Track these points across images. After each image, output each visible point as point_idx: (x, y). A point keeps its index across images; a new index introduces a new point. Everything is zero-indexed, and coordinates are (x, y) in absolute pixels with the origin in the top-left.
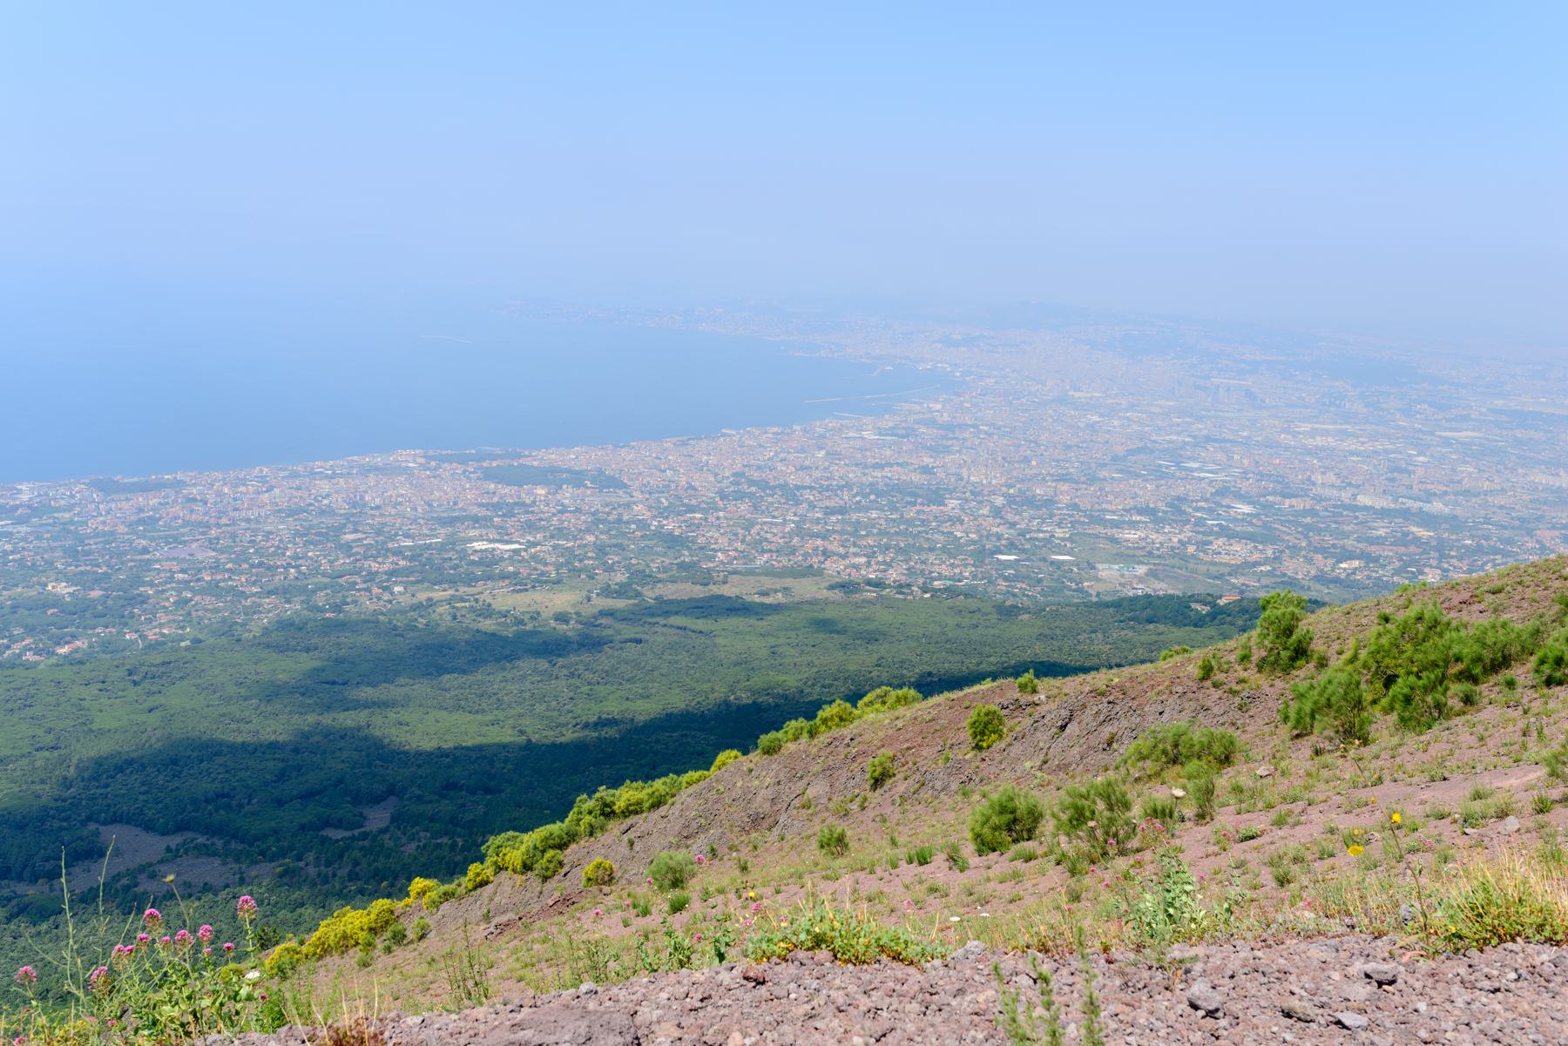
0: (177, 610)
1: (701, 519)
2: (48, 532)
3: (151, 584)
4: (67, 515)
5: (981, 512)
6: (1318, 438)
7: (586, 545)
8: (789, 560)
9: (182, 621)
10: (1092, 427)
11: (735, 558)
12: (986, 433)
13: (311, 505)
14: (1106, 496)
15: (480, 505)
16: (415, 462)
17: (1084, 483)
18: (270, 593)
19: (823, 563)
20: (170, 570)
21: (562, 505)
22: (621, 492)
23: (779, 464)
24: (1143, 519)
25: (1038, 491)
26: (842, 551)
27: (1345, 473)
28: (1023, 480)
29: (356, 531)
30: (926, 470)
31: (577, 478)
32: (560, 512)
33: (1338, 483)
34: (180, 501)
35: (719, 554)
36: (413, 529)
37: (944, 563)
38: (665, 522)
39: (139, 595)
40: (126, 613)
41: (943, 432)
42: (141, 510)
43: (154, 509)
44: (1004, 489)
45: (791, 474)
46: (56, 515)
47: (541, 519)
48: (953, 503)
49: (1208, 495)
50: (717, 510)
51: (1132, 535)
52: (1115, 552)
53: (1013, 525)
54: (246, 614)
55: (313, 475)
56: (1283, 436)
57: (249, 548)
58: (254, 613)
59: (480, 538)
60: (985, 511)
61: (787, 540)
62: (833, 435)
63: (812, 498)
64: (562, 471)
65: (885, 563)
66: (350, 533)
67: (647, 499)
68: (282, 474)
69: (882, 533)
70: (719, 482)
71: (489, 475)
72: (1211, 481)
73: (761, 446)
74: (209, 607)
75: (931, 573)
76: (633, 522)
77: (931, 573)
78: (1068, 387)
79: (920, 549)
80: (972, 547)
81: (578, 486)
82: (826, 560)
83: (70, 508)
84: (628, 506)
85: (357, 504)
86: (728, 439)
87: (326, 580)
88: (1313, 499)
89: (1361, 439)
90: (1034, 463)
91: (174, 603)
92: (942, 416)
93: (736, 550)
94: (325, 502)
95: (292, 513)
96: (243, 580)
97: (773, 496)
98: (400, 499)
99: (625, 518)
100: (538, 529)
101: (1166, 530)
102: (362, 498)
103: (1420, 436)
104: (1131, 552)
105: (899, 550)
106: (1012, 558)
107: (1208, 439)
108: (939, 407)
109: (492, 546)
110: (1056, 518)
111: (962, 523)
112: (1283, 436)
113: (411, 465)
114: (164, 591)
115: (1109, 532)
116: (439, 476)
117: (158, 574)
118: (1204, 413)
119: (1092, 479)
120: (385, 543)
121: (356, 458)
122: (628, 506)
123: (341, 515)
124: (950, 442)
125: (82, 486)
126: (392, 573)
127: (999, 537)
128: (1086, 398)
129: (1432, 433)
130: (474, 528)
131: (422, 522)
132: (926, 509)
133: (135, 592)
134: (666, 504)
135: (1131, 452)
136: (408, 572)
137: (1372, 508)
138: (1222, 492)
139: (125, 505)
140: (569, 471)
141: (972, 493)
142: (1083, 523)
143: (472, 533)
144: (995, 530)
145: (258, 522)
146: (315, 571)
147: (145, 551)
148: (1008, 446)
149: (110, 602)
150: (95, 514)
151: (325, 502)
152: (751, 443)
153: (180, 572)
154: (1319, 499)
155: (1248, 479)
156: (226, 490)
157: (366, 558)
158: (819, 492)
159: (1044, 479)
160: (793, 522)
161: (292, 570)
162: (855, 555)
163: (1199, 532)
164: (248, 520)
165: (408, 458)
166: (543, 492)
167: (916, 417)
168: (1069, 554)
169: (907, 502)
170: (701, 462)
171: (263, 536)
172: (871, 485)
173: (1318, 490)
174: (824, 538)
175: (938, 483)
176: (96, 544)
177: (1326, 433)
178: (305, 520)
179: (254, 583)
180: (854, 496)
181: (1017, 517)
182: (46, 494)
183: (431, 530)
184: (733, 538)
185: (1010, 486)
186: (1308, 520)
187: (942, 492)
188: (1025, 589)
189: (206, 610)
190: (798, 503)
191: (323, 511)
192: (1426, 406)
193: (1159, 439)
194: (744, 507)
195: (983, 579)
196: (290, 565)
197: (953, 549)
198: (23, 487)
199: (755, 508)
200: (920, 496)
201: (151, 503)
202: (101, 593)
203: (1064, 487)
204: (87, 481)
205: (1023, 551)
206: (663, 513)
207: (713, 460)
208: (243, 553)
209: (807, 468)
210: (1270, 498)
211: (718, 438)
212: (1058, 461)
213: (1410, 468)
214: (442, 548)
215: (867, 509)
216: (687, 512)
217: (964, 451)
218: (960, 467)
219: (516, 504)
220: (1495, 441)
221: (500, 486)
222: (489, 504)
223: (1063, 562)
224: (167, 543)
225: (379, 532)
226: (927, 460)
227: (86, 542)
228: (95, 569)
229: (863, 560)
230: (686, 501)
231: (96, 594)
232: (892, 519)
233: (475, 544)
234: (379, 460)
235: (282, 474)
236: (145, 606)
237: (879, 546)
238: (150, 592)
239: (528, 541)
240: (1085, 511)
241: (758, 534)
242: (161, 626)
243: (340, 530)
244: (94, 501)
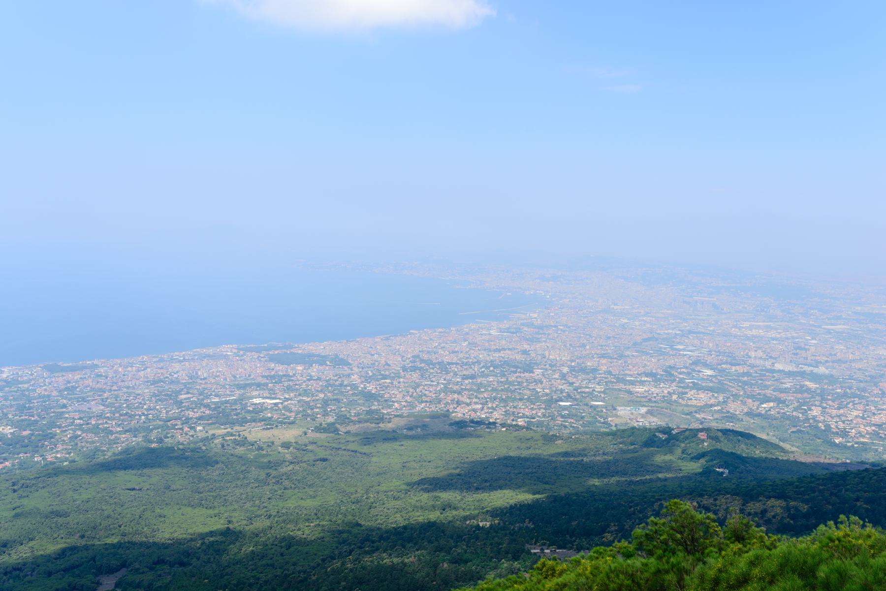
0: (70, 442)
1: (389, 383)
2: (12, 395)
3: (60, 427)
4: (26, 386)
5: (554, 376)
6: (754, 331)
7: (317, 400)
8: (436, 407)
9: (70, 449)
10: (623, 326)
11: (404, 406)
12: (561, 330)
13: (167, 377)
14: (628, 366)
15: (263, 377)
16: (231, 352)
17: (616, 358)
18: (126, 431)
19: (456, 408)
20: (73, 418)
21: (311, 376)
22: (346, 368)
23: (440, 350)
24: (648, 379)
25: (589, 364)
26: (468, 401)
27: (768, 350)
28: (580, 357)
29: (188, 393)
30: (525, 352)
31: (322, 360)
32: (309, 380)
33: (764, 356)
34: (92, 376)
35: (396, 404)
36: (221, 391)
37: (527, 407)
38: (368, 385)
39: (51, 433)
40: (40, 444)
41: (537, 330)
42: (69, 382)
43: (76, 382)
44: (569, 363)
45: (446, 356)
46: (20, 386)
47: (296, 385)
48: (538, 372)
49: (688, 365)
50: (399, 377)
51: (640, 389)
52: (629, 399)
53: (571, 384)
54: (109, 444)
55: (172, 360)
56: (733, 329)
57: (124, 404)
58: (115, 443)
59: (259, 396)
60: (557, 376)
61: (437, 395)
62: (473, 333)
63: (456, 370)
64: (314, 355)
65: (492, 408)
66: (186, 394)
67: (360, 372)
68: (155, 360)
69: (494, 390)
70: (404, 361)
71: (272, 359)
72: (690, 357)
73: (431, 339)
74: (90, 440)
75: (519, 413)
76: (349, 386)
77: (519, 413)
78: (611, 303)
79: (515, 399)
80: (545, 398)
81: (321, 364)
82: (457, 407)
83: (28, 382)
84: (349, 376)
85: (193, 377)
86: (413, 336)
87: (161, 423)
88: (749, 366)
89: (779, 331)
90: (588, 347)
91: (70, 438)
92: (537, 321)
93: (406, 401)
94: (176, 376)
95: (154, 383)
96: (114, 423)
97: (433, 369)
98: (218, 374)
99: (345, 383)
100: (293, 391)
101: (661, 386)
102: (197, 373)
103: (813, 328)
104: (639, 399)
105: (502, 400)
106: (568, 404)
107: (690, 332)
108: (536, 315)
109: (264, 401)
110: (597, 380)
111: (542, 383)
112: (733, 329)
113: (228, 353)
114: (66, 431)
115: (627, 387)
116: (244, 360)
117: (65, 421)
118: (688, 317)
119: (621, 356)
120: (203, 400)
121: (198, 350)
122: (349, 376)
123: (183, 383)
124: (540, 336)
125: (39, 369)
126: (200, 418)
127: (562, 391)
128: (621, 309)
129: (820, 327)
130: (256, 390)
131: (227, 387)
132: (522, 375)
133: (49, 432)
134: (371, 374)
135: (645, 340)
136: (210, 417)
137: (783, 371)
139: (61, 379)
140: (318, 356)
141: (550, 365)
142: (613, 382)
143: (255, 393)
144: (560, 387)
145: (134, 388)
146: (157, 418)
147: (64, 406)
148: (574, 337)
149: (33, 438)
150: (42, 385)
151: (176, 376)
152: (426, 338)
153: (79, 419)
154: (752, 366)
155: (711, 355)
156: (120, 370)
157: (188, 409)
158: (461, 366)
159: (592, 356)
160: (443, 384)
161: (143, 417)
162: (476, 403)
163: (681, 387)
164: (128, 387)
165: (228, 349)
166: (301, 368)
167: (522, 322)
168: (602, 401)
169: (512, 371)
170: (396, 349)
171: (134, 397)
172: (492, 361)
173: (752, 361)
174: (459, 393)
175: (531, 360)
176: (37, 402)
177: (759, 327)
178: (161, 387)
179: (119, 425)
180: (481, 368)
181: (575, 379)
182: (17, 373)
183: (231, 391)
184: (407, 394)
185: (572, 361)
186: (745, 379)
187: (532, 365)
188: (573, 423)
189: (87, 442)
190: (447, 373)
191: (173, 382)
192: (816, 311)
193: (662, 332)
194: (415, 376)
195: (549, 416)
196: (143, 414)
197: (534, 399)
198: (6, 370)
199: (422, 376)
200: (520, 368)
201: (75, 378)
202: (29, 432)
203: (604, 361)
204: (42, 365)
205: (575, 399)
206: (368, 379)
207: (402, 348)
208: (120, 407)
209: (456, 352)
211: (407, 335)
212: (602, 346)
213: (807, 347)
214: (235, 402)
215: (488, 376)
216: (382, 379)
217: (548, 341)
218: (544, 350)
219: (284, 375)
220: (857, 331)
221: (277, 365)
222: (268, 376)
223: (598, 406)
224: (78, 401)
225: (201, 394)
226: (526, 347)
227: (32, 401)
228: (30, 418)
229: (480, 406)
230: (383, 372)
231: (26, 433)
232: (501, 382)
233: (254, 400)
234: (211, 351)
235: (155, 360)
236: (52, 440)
237: (490, 398)
238: (58, 432)
239: (285, 398)
240: (615, 375)
241: (421, 391)
242: (57, 452)
243: (179, 392)
244: (43, 377)
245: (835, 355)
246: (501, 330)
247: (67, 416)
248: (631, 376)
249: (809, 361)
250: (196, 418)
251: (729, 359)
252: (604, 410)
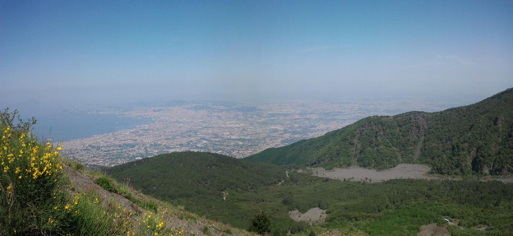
10: (180, 127)
25: (159, 143)
41: (144, 131)
90: (162, 136)
107: (205, 127)
135: (186, 132)
137: (233, 139)
141: (143, 144)
173: (223, 136)
203: (165, 141)
210: (212, 139)
213: (247, 129)
245: (256, 131)
246: (130, 133)
248: (173, 146)
249: (245, 135)
251: (215, 136)
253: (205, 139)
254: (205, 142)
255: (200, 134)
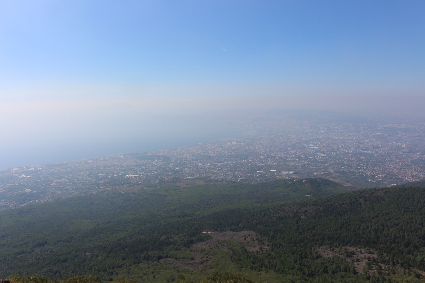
29: (101, 174)
72: (315, 149)
138: (318, 151)
142: (281, 161)
233: (128, 175)
247: (52, 184)
250: (102, 183)
252: (275, 173)
253: (321, 152)
254: (323, 155)
255: (313, 146)
